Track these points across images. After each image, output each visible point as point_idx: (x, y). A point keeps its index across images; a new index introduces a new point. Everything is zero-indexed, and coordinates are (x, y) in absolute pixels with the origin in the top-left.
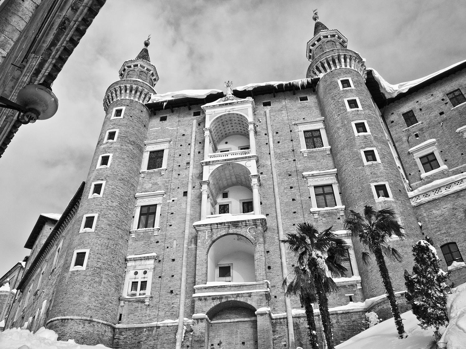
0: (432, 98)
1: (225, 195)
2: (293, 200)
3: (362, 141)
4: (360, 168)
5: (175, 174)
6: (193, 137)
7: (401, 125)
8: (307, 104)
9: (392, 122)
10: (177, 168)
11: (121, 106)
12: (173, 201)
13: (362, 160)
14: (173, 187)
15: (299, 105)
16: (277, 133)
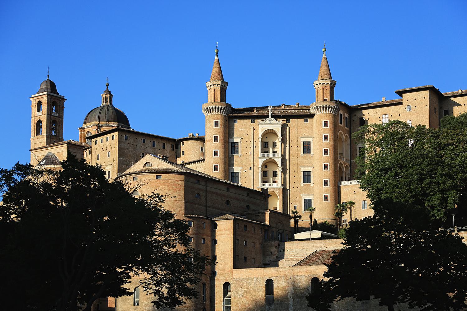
0: (375, 114)
1: (266, 167)
2: (295, 177)
3: (324, 159)
4: (322, 171)
5: (245, 157)
6: (252, 138)
7: (357, 125)
8: (307, 124)
9: (354, 121)
10: (246, 154)
11: (217, 119)
12: (245, 171)
13: (322, 168)
14: (245, 164)
15: (304, 125)
16: (291, 141)
